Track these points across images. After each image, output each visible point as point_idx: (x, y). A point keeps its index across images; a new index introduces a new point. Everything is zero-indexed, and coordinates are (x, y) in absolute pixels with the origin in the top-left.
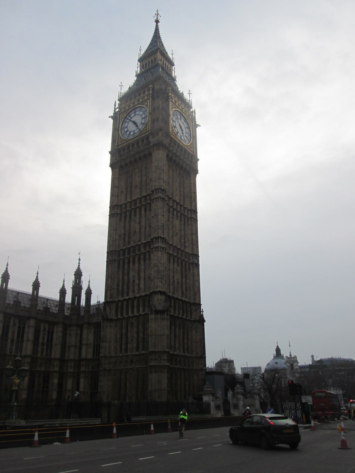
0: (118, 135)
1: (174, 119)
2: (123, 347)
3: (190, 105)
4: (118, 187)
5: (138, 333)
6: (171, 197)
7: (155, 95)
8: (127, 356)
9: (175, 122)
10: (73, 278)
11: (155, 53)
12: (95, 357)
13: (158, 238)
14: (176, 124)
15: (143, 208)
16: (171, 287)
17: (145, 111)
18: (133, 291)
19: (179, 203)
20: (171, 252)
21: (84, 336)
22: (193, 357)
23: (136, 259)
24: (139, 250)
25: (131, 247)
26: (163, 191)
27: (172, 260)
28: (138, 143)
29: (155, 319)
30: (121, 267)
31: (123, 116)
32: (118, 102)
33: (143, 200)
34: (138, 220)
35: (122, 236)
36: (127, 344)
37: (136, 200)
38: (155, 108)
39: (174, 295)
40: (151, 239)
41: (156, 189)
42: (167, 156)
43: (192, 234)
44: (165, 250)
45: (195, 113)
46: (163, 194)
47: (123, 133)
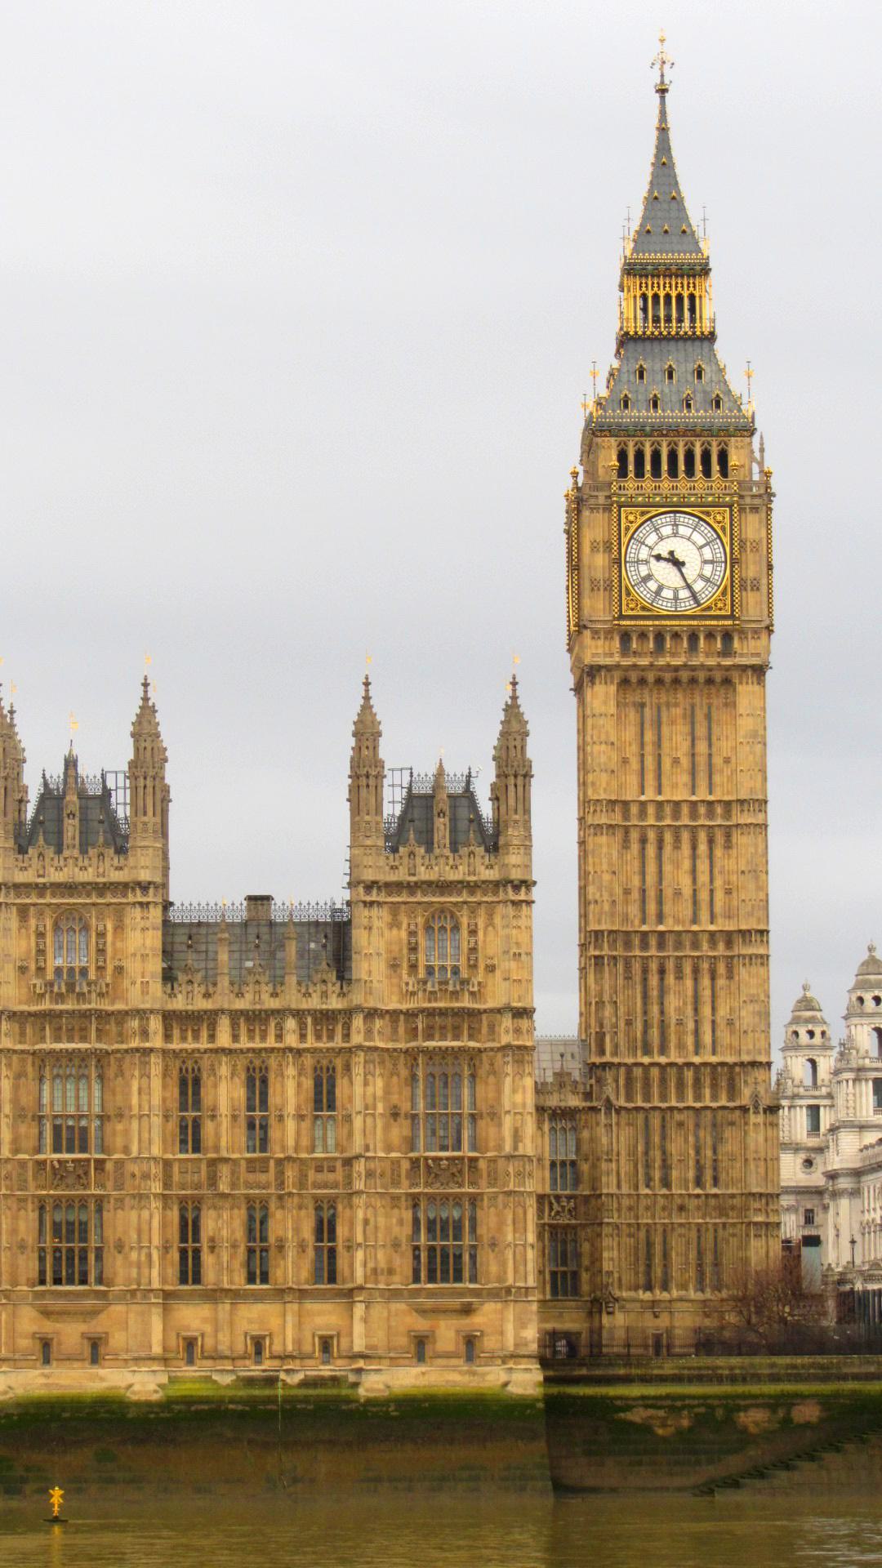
5: (698, 1151)
7: (748, 500)
12: (559, 1192)
15: (702, 836)
18: (681, 1046)
23: (688, 969)
24: (696, 945)
28: (693, 638)
30: (638, 978)
31: (631, 518)
33: (702, 810)
34: (686, 864)
35: (636, 895)
36: (666, 1166)
37: (677, 804)
47: (634, 579)
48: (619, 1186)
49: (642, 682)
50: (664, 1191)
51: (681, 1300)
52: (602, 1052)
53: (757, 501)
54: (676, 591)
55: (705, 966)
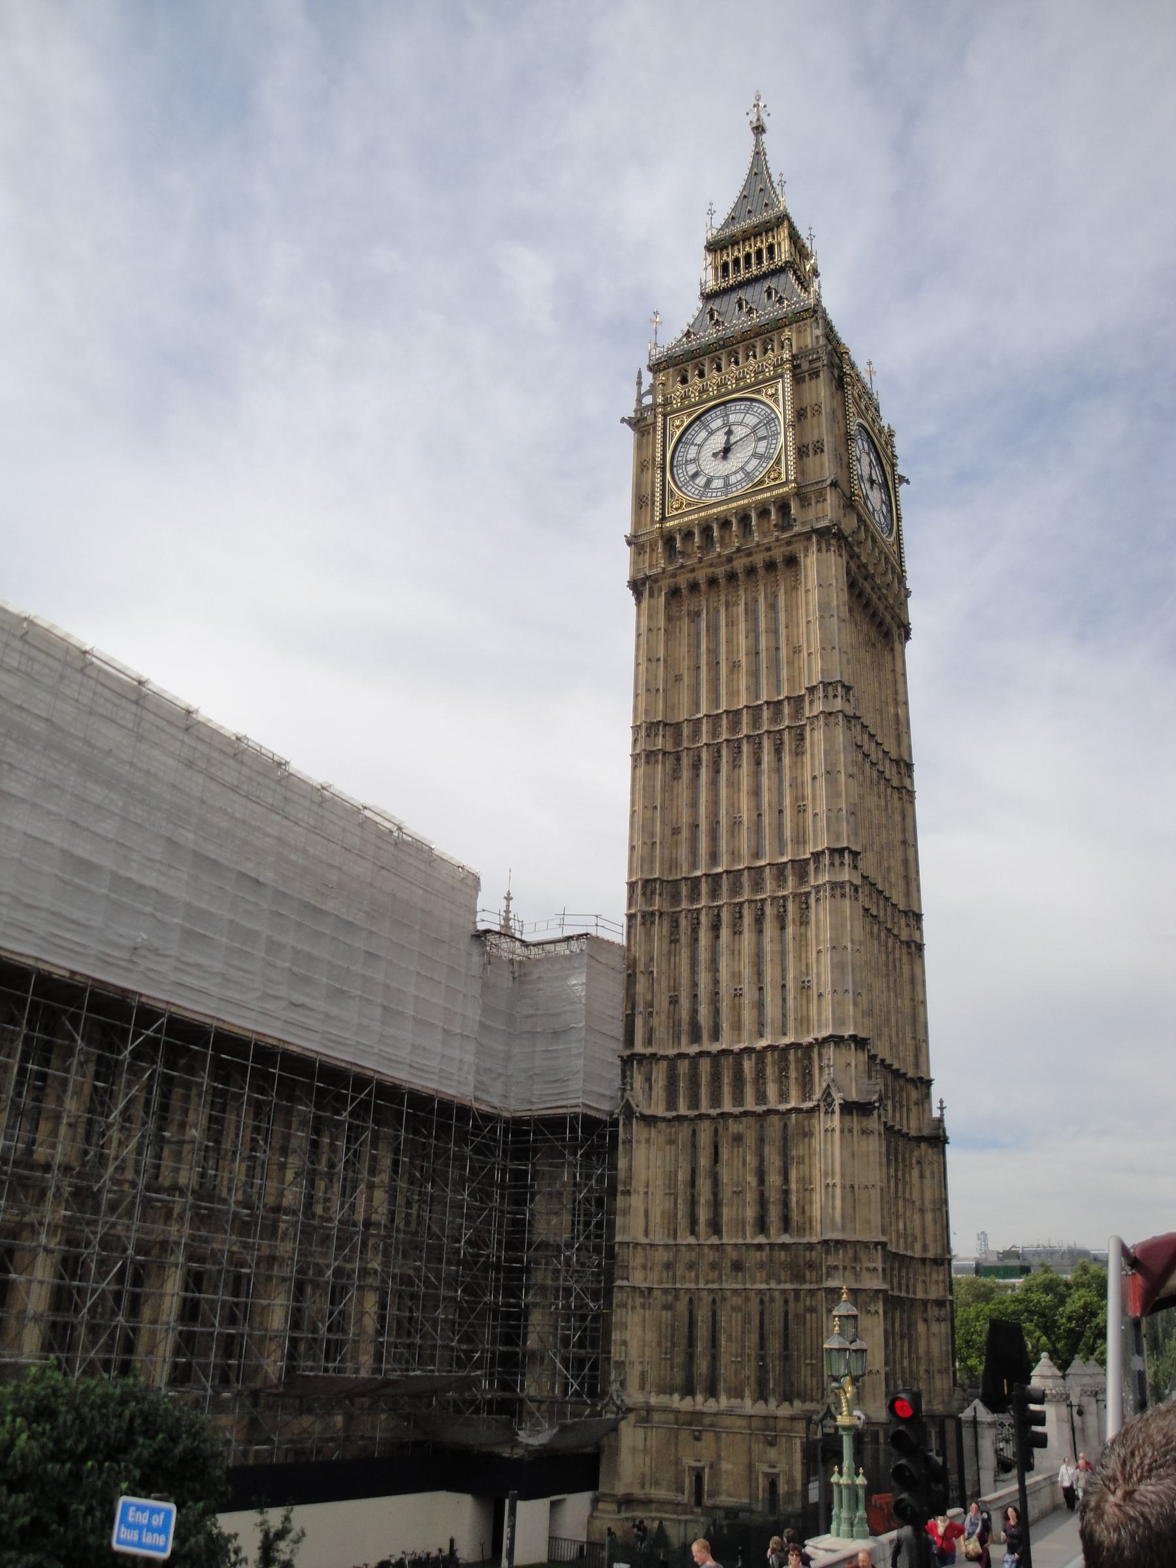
0: (663, 485)
2: (703, 1215)
7: (805, 366)
8: (719, 1248)
11: (772, 230)
13: (841, 851)
18: (737, 1026)
24: (758, 886)
26: (847, 693)
28: (744, 520)
30: (684, 940)
31: (678, 423)
32: (648, 378)
34: (745, 783)
35: (685, 834)
36: (716, 1204)
37: (739, 712)
41: (826, 685)
43: (904, 842)
48: (646, 1234)
49: (694, 587)
50: (714, 1240)
51: (730, 1413)
52: (629, 1040)
53: (816, 365)
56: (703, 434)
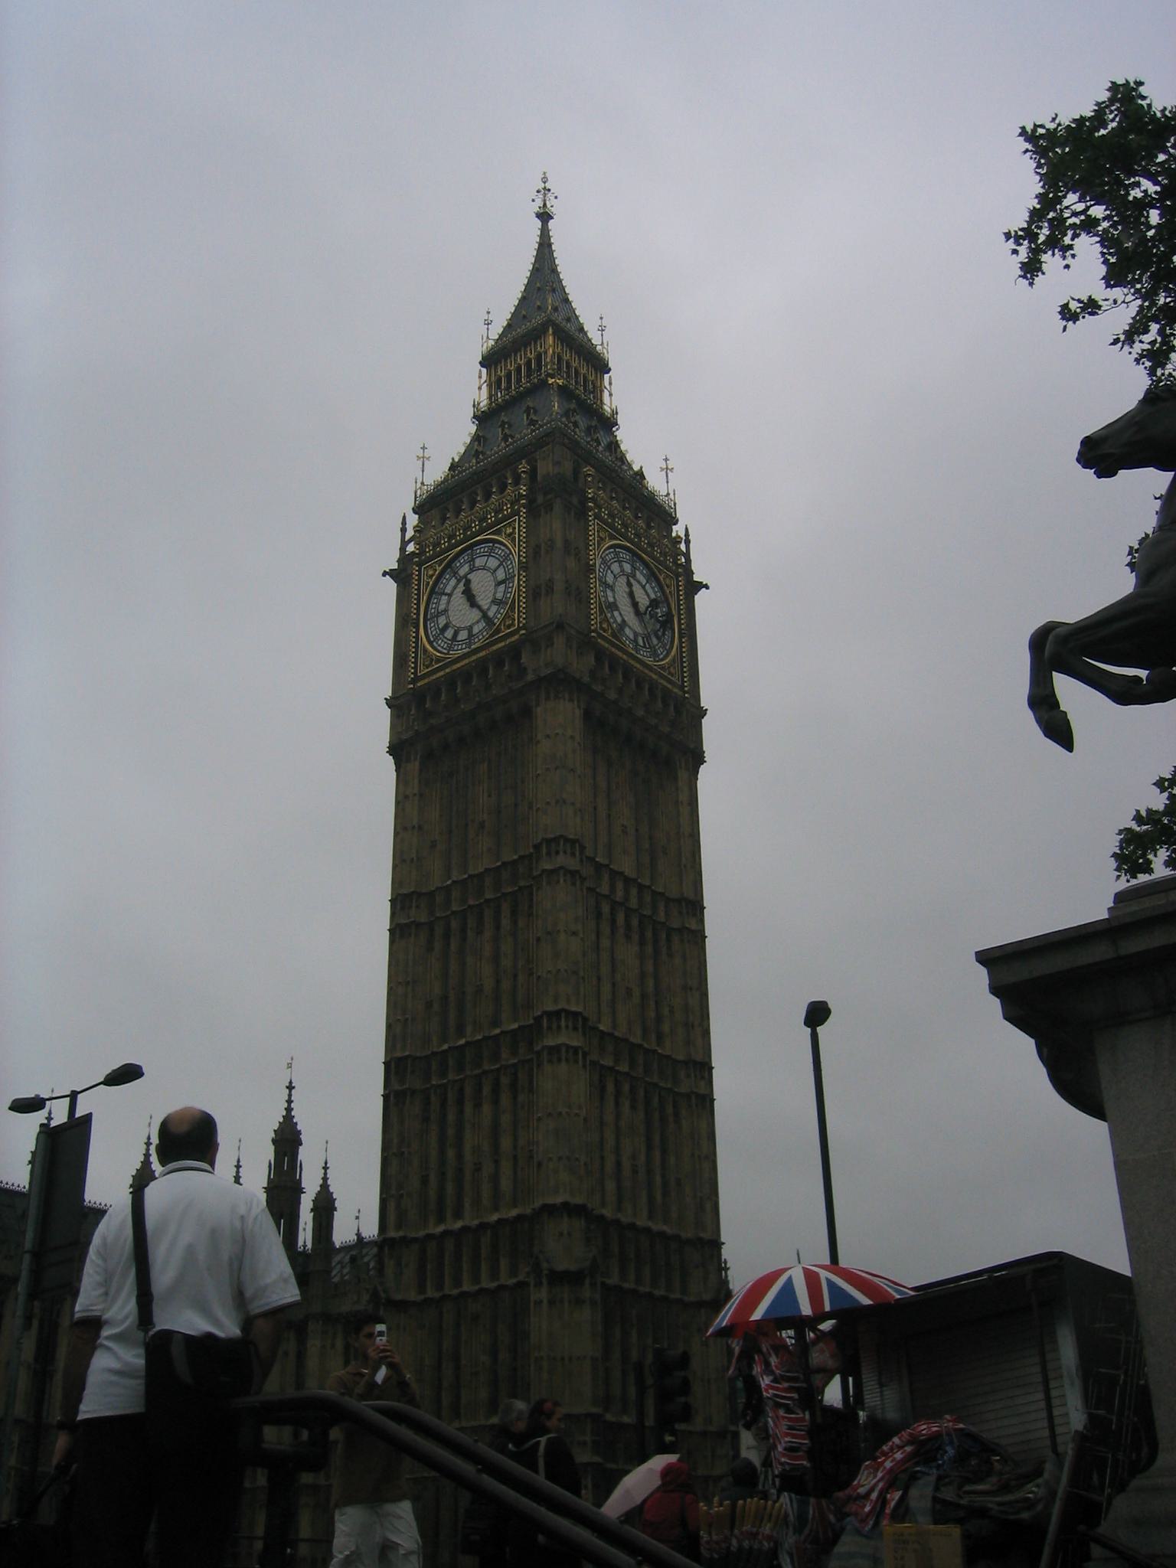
0: (416, 643)
1: (610, 579)
3: (670, 515)
4: (420, 828)
6: (605, 861)
9: (613, 590)
10: (269, 1153)
13: (557, 1014)
14: (622, 592)
16: (610, 1186)
17: (506, 558)
19: (635, 880)
20: (608, 1061)
21: (312, 1363)
22: (690, 1432)
23: (486, 1090)
25: (468, 1043)
27: (610, 1088)
29: (551, 1303)
35: (436, 1007)
38: (538, 546)
39: (619, 1215)
40: (535, 1019)
41: (548, 841)
42: (587, 715)
44: (585, 1055)
45: (688, 542)
46: (573, 854)
54: (470, 629)
55: (505, 1080)
56: (453, 582)
